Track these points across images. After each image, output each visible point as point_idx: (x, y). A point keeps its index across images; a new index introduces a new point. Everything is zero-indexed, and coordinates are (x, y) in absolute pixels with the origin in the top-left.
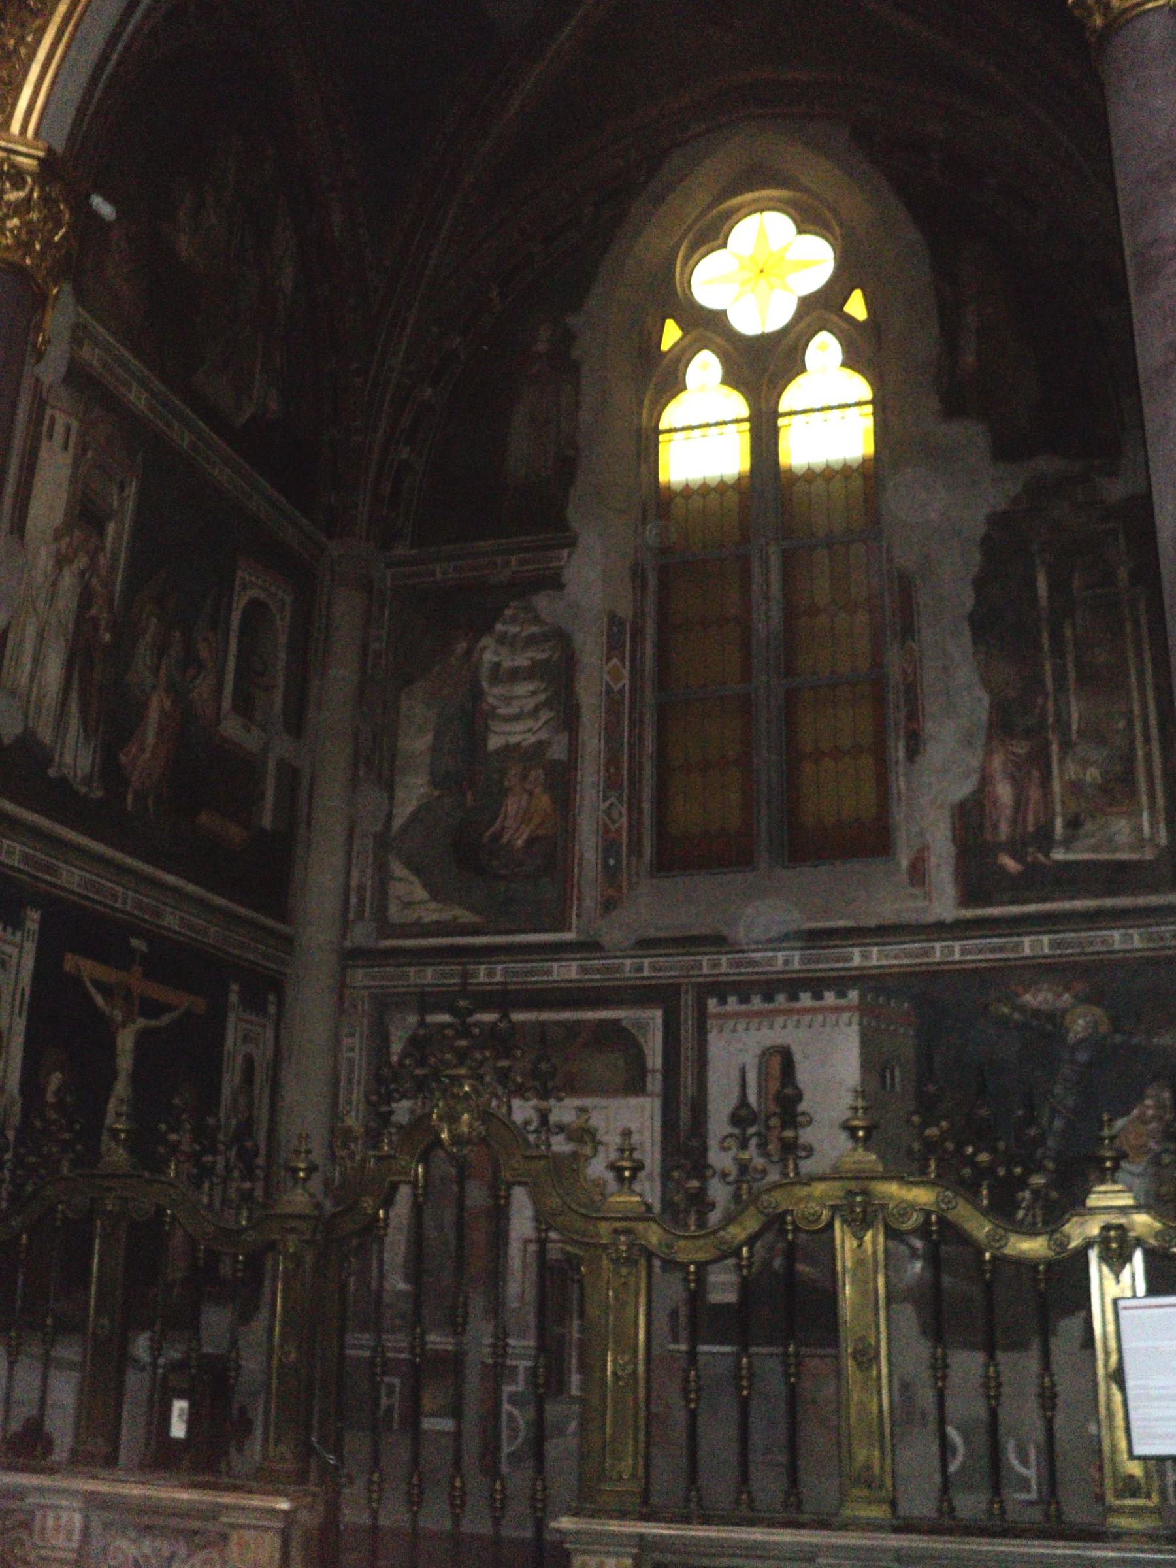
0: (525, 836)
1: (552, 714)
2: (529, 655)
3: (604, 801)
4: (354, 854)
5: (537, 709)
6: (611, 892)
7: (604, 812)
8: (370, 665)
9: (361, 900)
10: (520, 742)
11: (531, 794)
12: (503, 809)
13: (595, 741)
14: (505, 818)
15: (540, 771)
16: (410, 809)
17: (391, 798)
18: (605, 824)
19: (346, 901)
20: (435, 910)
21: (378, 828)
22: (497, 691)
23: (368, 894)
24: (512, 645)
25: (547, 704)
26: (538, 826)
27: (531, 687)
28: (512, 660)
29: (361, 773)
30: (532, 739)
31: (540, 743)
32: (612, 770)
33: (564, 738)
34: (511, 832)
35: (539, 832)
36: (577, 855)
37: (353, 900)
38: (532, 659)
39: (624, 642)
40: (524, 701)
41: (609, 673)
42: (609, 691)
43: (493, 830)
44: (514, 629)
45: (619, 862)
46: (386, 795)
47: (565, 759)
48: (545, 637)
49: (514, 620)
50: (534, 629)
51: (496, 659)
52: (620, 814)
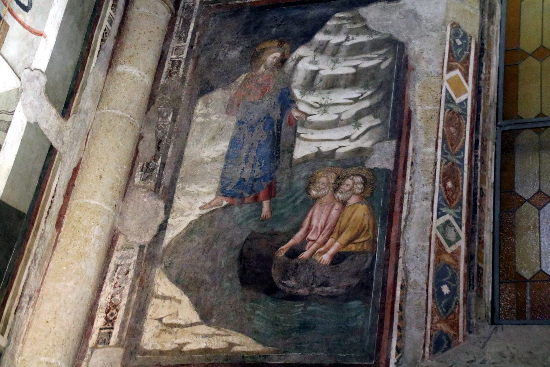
0: (332, 251)
1: (378, 121)
2: (355, 63)
3: (438, 217)
4: (112, 267)
5: (359, 116)
6: (444, 327)
7: (438, 228)
8: (164, 75)
9: (109, 322)
10: (336, 149)
11: (344, 204)
12: (307, 220)
13: (432, 149)
14: (308, 230)
15: (359, 179)
16: (193, 218)
17: (168, 209)
18: (440, 244)
19: (90, 319)
20: (206, 336)
21: (147, 239)
22: (312, 99)
23: (120, 315)
24: (334, 54)
25: (371, 111)
26: (350, 242)
27: (354, 93)
28: (332, 69)
29: (137, 180)
30: (350, 146)
31: (360, 150)
32: (449, 184)
33: (390, 146)
34: (315, 246)
35: (352, 247)
36: (401, 274)
37: (99, 322)
38: (356, 67)
39: (468, 58)
40: (341, 109)
41: (448, 81)
42: (449, 100)
43: (291, 242)
44: (335, 40)
45: (454, 291)
46: (162, 204)
47: (390, 166)
48: (375, 46)
49: (338, 30)
50: (363, 38)
51: (315, 68)
52: (458, 238)
